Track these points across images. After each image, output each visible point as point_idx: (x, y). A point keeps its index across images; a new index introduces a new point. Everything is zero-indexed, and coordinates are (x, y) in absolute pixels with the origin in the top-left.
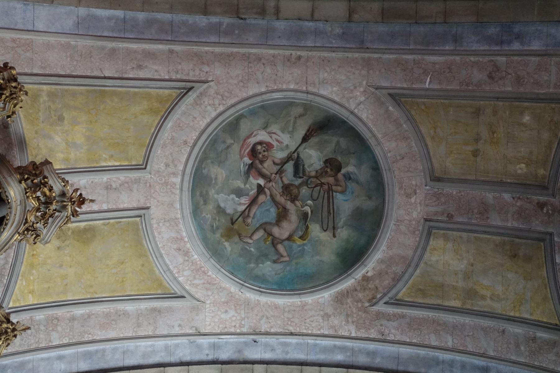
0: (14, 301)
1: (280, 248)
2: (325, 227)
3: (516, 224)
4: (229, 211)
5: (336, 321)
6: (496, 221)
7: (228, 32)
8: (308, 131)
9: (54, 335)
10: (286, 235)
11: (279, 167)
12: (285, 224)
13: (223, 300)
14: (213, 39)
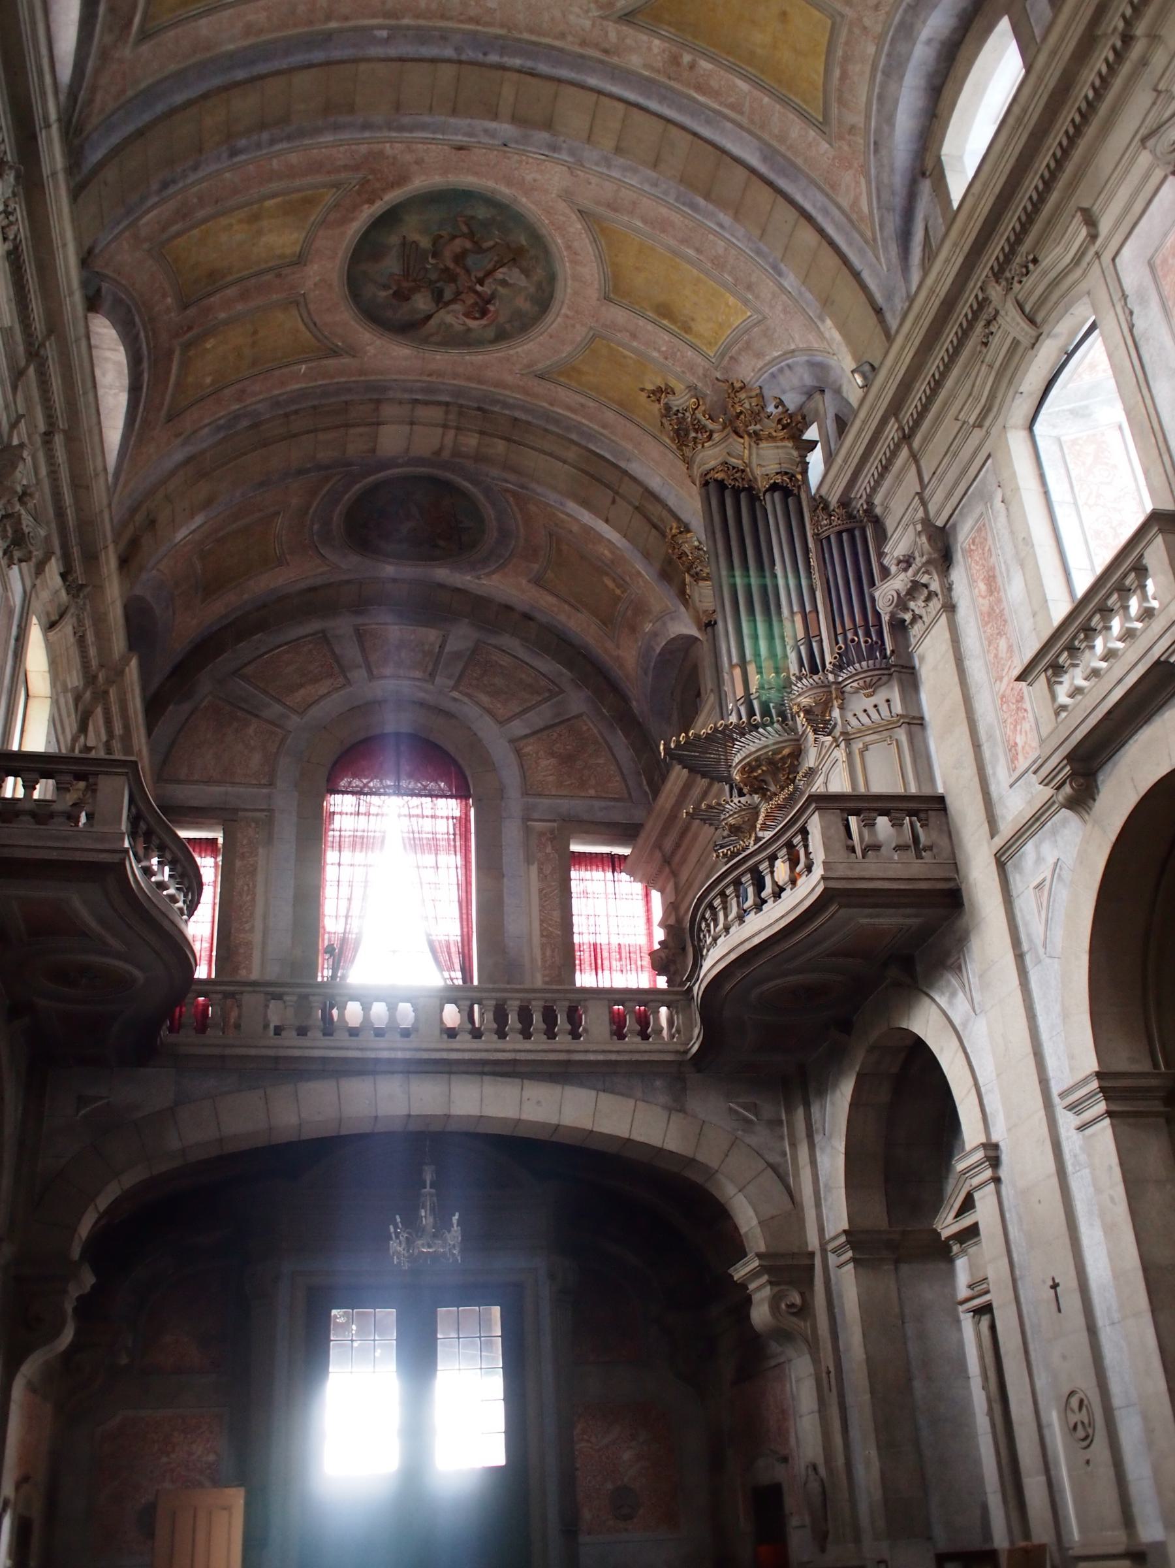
0: (746, 313)
1: (465, 229)
2: (414, 245)
3: (212, 299)
4: (516, 271)
5: (408, 157)
6: (231, 292)
7: (496, 402)
8: (425, 324)
9: (721, 251)
10: (458, 241)
11: (460, 297)
12: (458, 250)
13: (536, 193)
14: (511, 401)
